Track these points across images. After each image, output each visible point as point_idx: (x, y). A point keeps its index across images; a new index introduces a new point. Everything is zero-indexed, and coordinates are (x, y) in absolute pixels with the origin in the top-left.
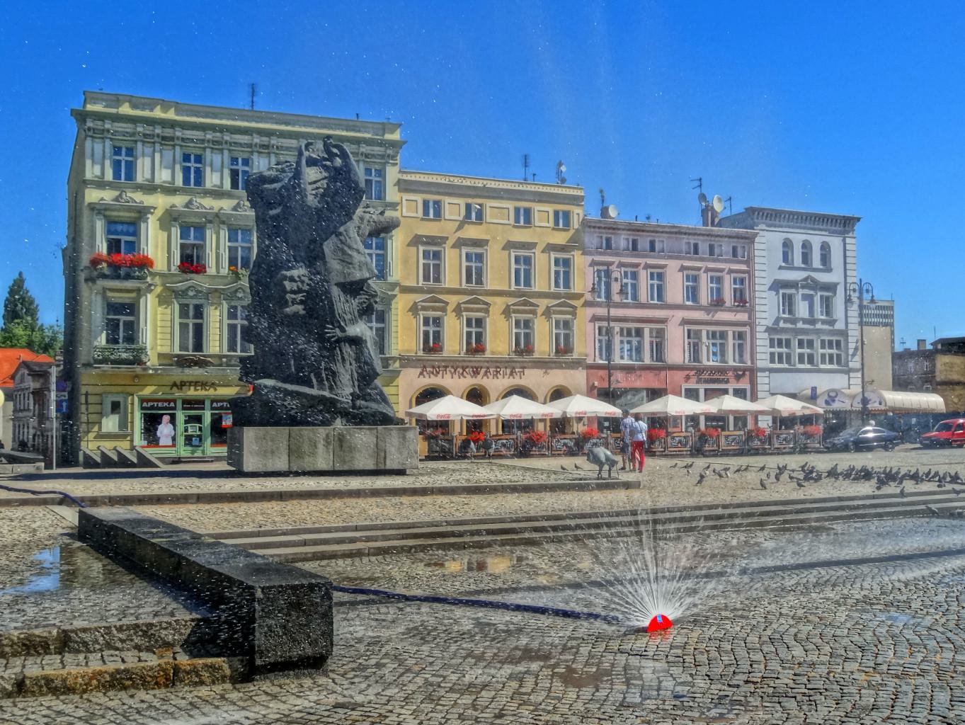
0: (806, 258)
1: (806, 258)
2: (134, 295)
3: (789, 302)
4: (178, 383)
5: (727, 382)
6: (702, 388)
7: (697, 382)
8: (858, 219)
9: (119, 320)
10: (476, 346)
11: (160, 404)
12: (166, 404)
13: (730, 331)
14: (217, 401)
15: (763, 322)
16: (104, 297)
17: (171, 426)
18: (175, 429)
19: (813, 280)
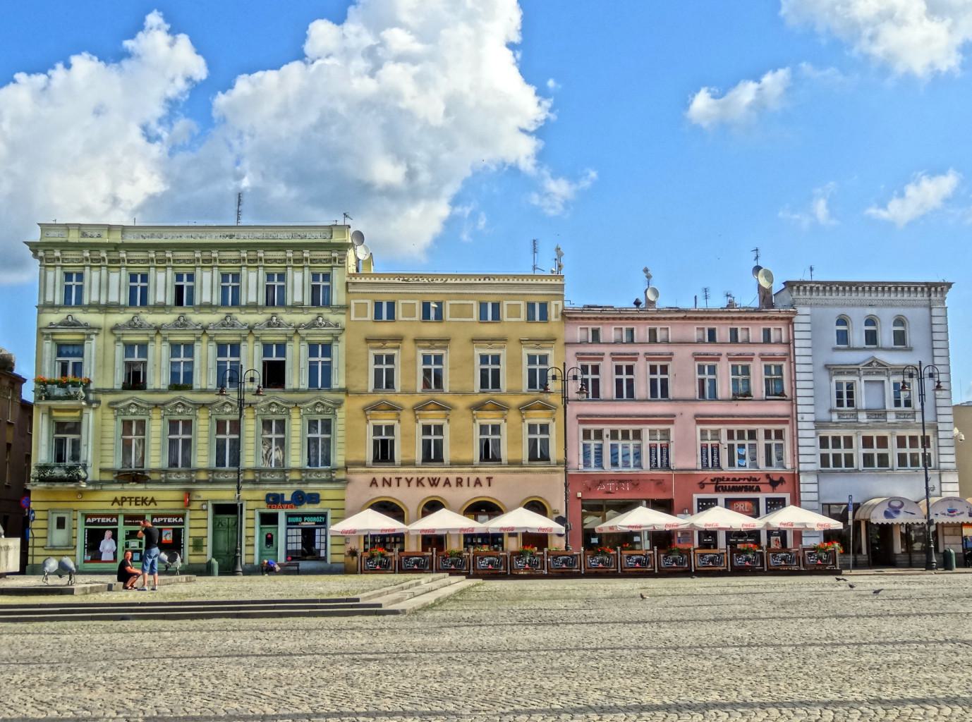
0: (871, 338)
1: (871, 338)
2: (77, 414)
4: (119, 499)
5: (758, 490)
6: (721, 497)
7: (717, 490)
8: (949, 285)
9: (65, 438)
10: (433, 454)
11: (103, 520)
12: (108, 520)
13: (760, 429)
14: (158, 516)
15: (807, 417)
16: (50, 417)
17: (113, 541)
18: (116, 545)
19: (879, 364)
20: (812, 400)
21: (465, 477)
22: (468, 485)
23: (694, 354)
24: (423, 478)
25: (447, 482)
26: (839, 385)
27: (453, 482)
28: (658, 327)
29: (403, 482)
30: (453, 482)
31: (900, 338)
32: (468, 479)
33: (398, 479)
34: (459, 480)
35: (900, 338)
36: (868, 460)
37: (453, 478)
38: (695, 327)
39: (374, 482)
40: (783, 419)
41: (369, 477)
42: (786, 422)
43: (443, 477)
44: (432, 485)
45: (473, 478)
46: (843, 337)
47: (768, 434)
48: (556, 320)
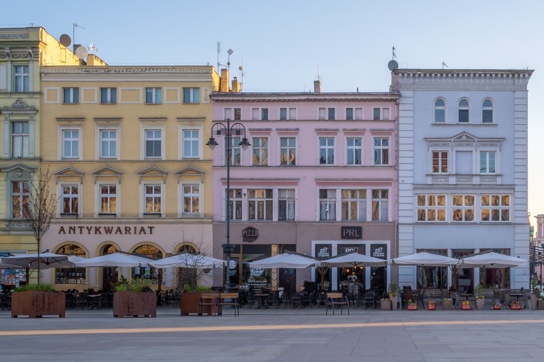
0: (464, 116)
1: (464, 116)
3: (440, 160)
8: (529, 73)
20: (413, 166)
21: (132, 226)
22: (135, 233)
23: (316, 130)
24: (100, 227)
25: (119, 230)
26: (436, 155)
27: (123, 230)
28: (287, 106)
29: (85, 231)
30: (123, 230)
31: (487, 116)
32: (135, 228)
33: (81, 228)
34: (128, 229)
35: (487, 116)
36: (457, 214)
37: (122, 227)
38: (318, 107)
39: (62, 229)
40: (388, 181)
41: (58, 227)
42: (390, 184)
43: (115, 227)
44: (107, 233)
45: (139, 227)
46: (440, 115)
47: (375, 193)
48: (206, 102)
